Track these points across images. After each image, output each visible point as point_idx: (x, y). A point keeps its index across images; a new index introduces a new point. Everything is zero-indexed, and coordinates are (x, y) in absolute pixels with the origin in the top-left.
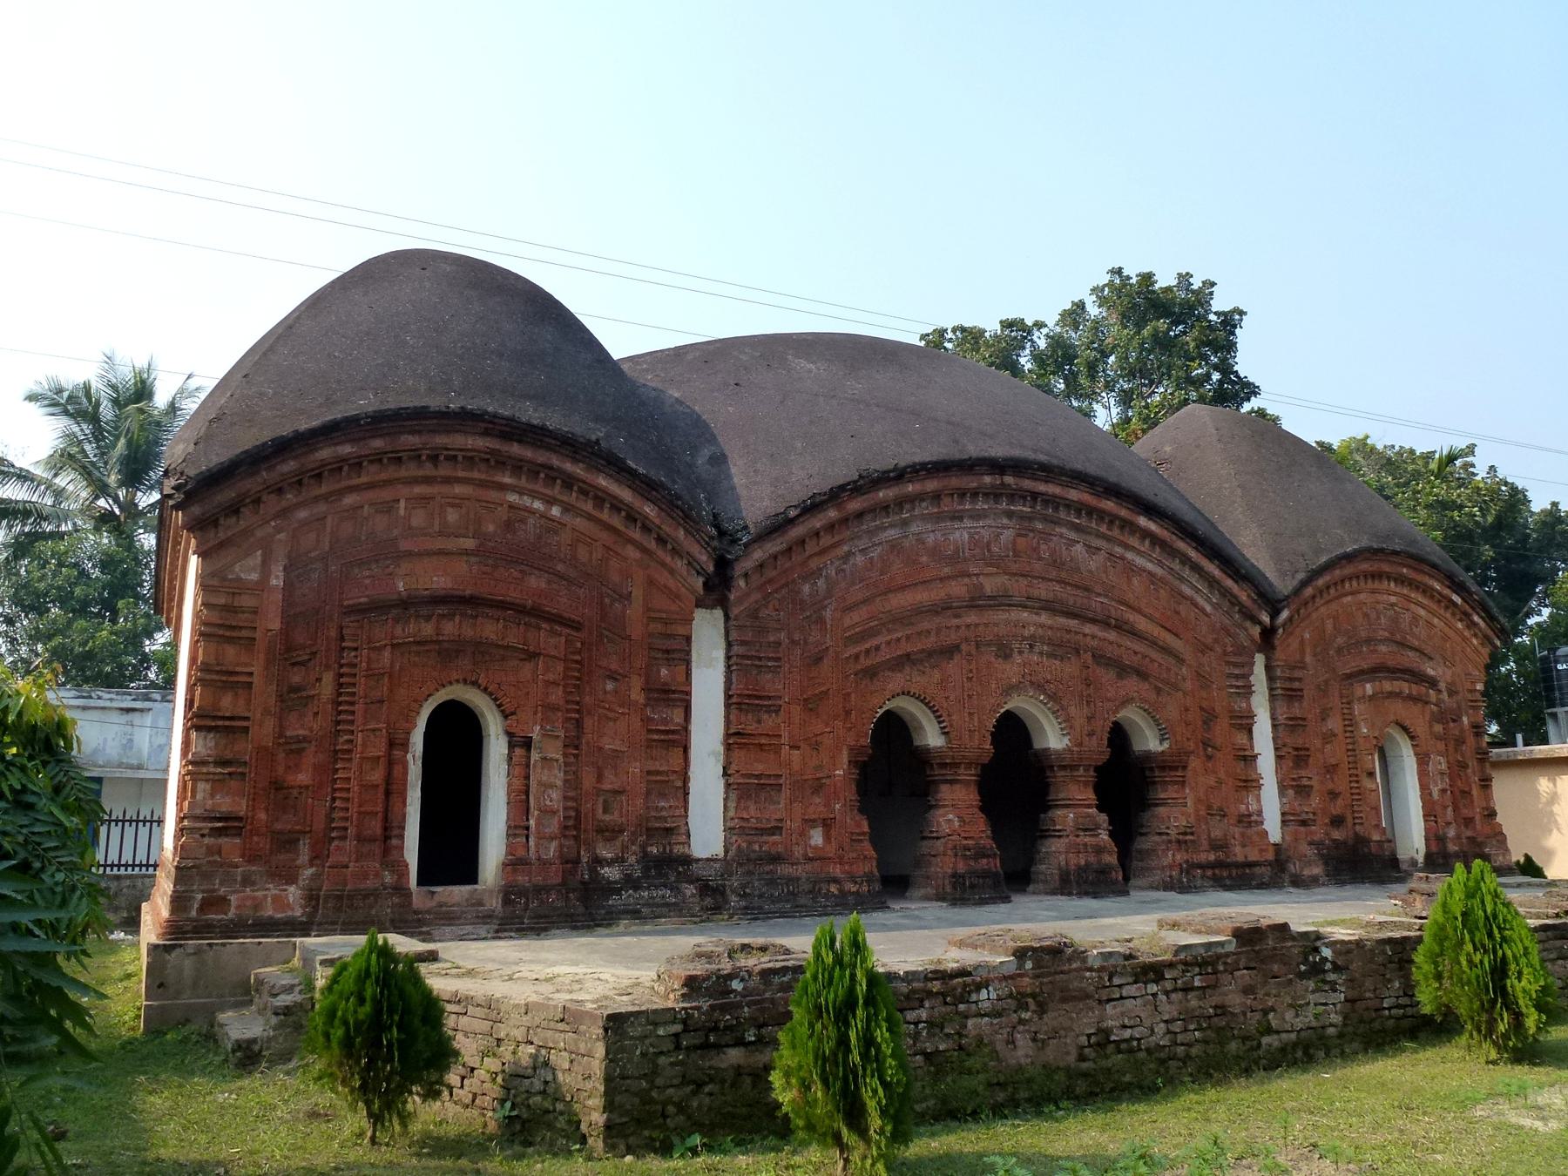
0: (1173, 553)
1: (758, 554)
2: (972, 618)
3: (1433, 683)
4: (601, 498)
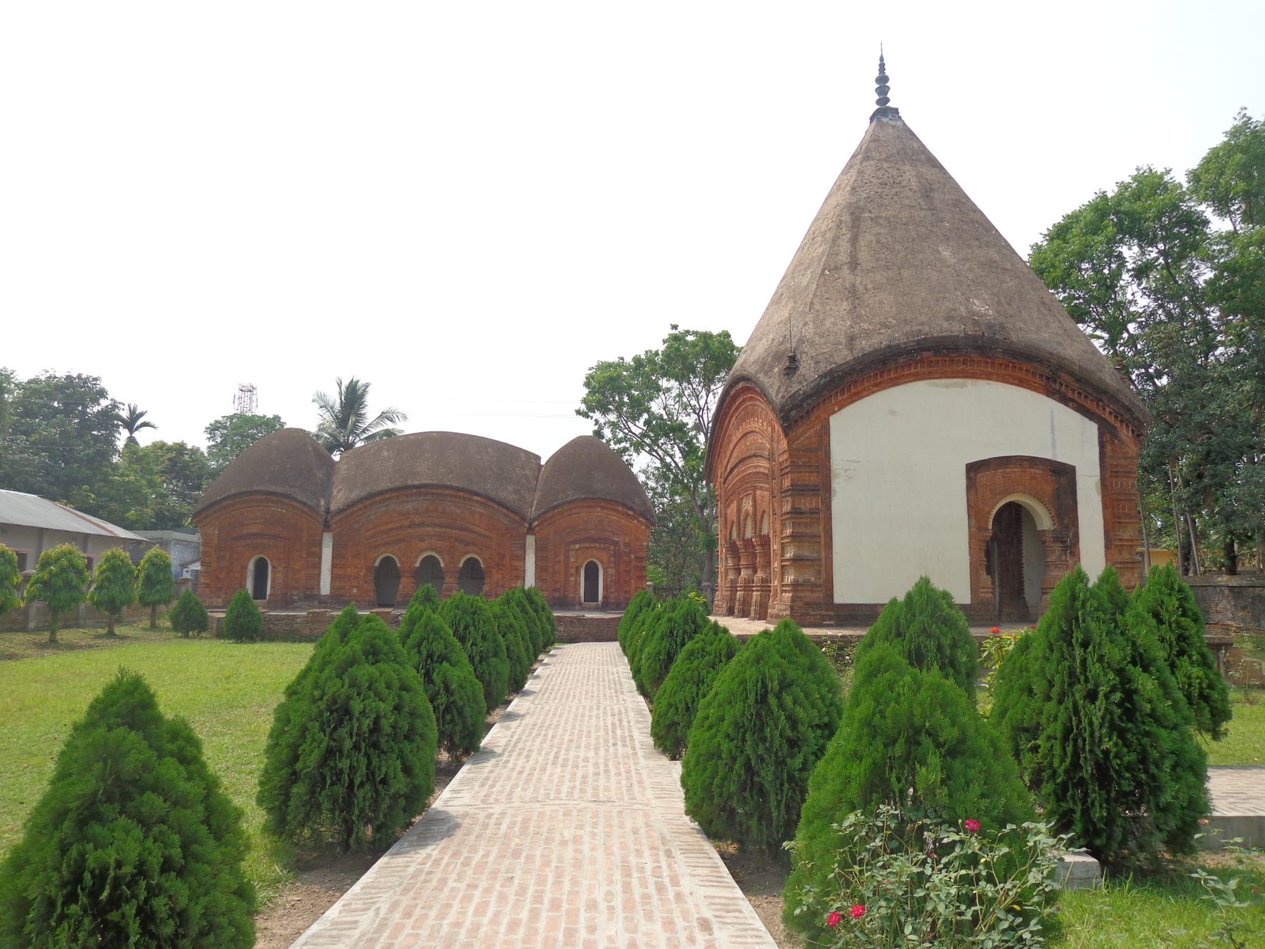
0: (490, 506)
1: (337, 518)
2: (410, 530)
3: (616, 543)
4: (294, 508)
